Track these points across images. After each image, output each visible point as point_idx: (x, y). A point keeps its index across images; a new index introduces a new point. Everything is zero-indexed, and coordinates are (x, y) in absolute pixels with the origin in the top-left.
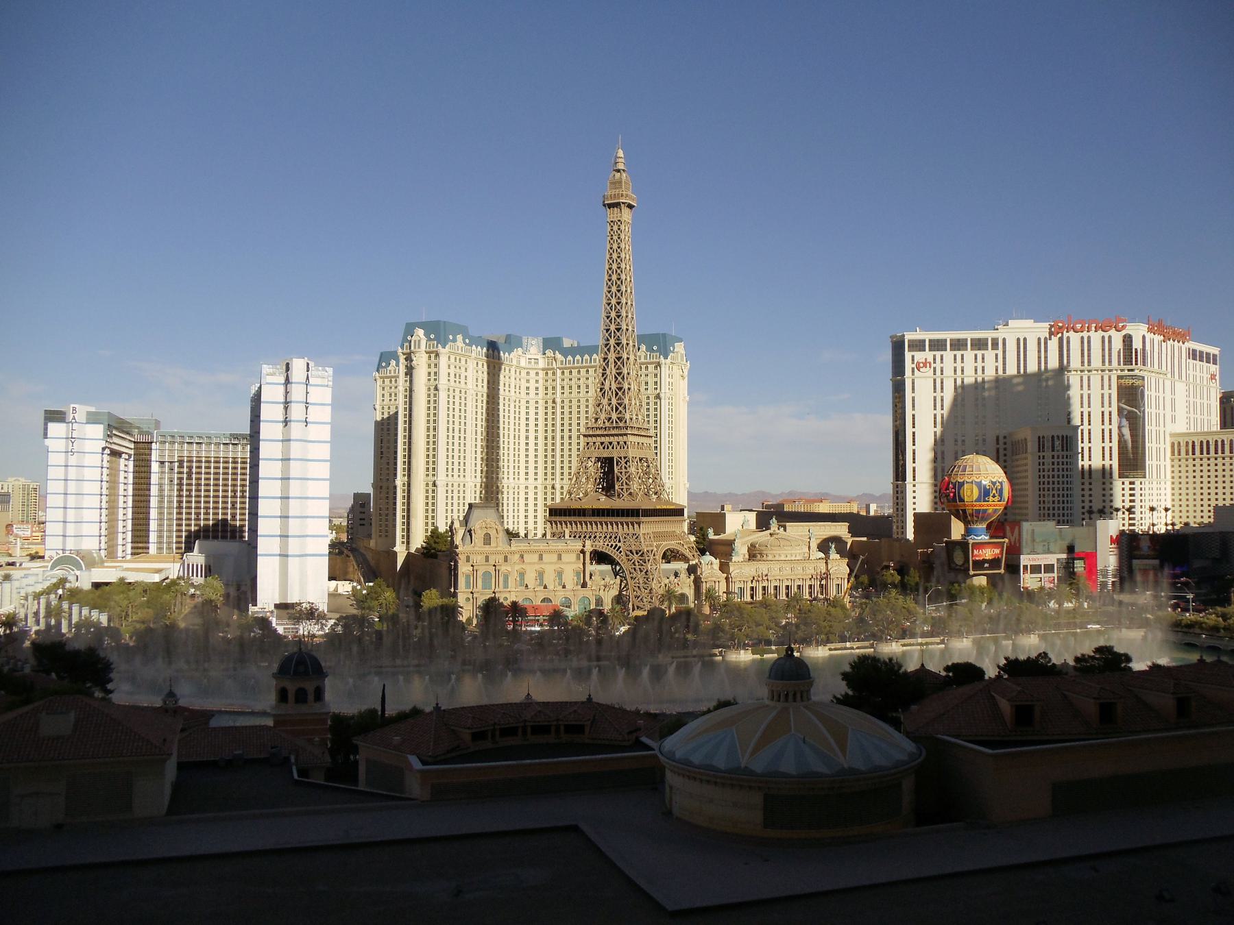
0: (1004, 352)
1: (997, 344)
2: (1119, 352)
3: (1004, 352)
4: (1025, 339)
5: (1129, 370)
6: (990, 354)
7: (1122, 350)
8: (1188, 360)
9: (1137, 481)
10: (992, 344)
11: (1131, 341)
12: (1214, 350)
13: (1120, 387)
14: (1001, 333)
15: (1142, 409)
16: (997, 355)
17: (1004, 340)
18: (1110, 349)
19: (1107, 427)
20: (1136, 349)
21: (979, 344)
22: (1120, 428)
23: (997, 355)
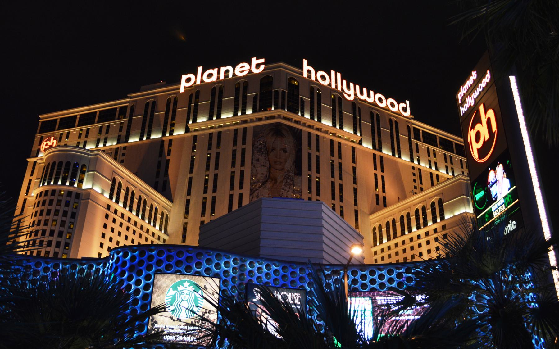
0: (130, 120)
2: (255, 97)
3: (130, 120)
5: (268, 118)
18: (245, 97)
19: (236, 192)
20: (277, 92)
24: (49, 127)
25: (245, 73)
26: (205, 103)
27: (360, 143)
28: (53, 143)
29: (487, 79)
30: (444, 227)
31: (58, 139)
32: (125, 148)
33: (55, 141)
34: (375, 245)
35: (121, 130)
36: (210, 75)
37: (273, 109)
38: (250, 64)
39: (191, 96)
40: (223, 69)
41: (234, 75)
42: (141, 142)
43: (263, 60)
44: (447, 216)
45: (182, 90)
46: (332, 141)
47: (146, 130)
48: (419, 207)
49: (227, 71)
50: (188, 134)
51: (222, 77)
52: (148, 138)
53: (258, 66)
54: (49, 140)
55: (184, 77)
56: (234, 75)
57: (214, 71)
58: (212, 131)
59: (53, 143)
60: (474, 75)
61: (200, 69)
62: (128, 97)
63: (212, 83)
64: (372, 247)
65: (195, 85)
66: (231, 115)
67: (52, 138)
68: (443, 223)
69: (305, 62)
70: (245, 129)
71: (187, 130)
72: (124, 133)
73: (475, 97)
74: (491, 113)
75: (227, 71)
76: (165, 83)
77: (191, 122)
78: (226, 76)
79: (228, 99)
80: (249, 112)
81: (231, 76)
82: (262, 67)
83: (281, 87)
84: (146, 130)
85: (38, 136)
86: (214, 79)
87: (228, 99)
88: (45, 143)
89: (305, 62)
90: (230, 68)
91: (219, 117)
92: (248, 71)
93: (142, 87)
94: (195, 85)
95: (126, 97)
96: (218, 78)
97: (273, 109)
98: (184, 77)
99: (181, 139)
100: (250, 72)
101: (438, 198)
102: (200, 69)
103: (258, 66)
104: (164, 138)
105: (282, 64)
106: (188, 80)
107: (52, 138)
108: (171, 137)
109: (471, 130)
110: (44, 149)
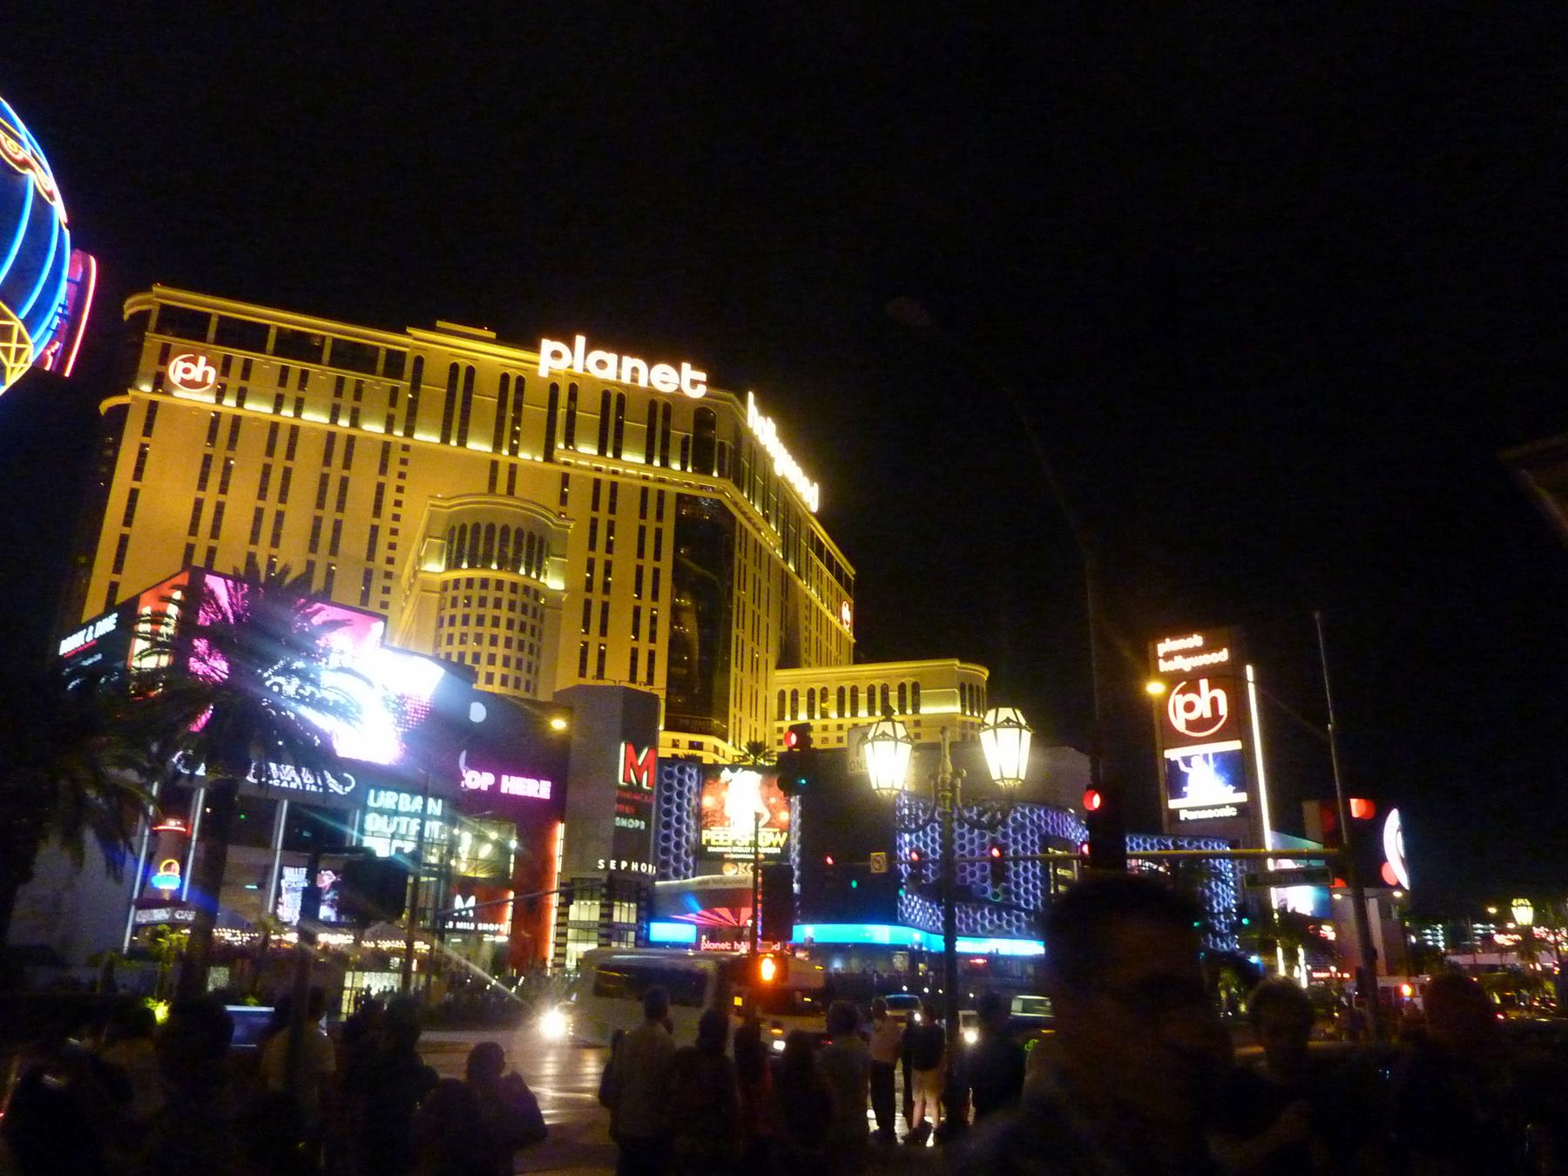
0: (415, 388)
1: (401, 365)
2: (685, 441)
4: (471, 371)
6: (378, 384)
7: (691, 440)
8: (809, 549)
9: (709, 741)
10: (388, 363)
11: (711, 425)
12: (850, 570)
13: (680, 521)
14: (414, 340)
15: (729, 583)
16: (394, 392)
17: (419, 361)
18: (666, 435)
20: (722, 445)
21: (352, 357)
22: (676, 611)
23: (394, 392)
24: (190, 326)
25: (669, 389)
26: (588, 415)
27: (775, 550)
28: (205, 374)
29: (1223, 656)
30: (917, 723)
31: (220, 366)
32: (406, 448)
33: (212, 372)
34: (781, 717)
35: (393, 402)
36: (601, 364)
37: (715, 474)
38: (678, 369)
39: (554, 388)
40: (629, 363)
41: (650, 383)
42: (444, 447)
43: (702, 376)
44: (926, 709)
45: (543, 372)
46: (756, 540)
47: (455, 425)
48: (878, 683)
49: (635, 370)
50: (548, 466)
52: (462, 442)
53: (694, 383)
54: (195, 363)
55: (548, 345)
56: (650, 383)
57: (611, 358)
58: (598, 475)
59: (205, 374)
60: (1197, 640)
61: (580, 341)
62: (409, 335)
63: (605, 382)
64: (775, 720)
65: (569, 370)
66: (641, 460)
67: (202, 360)
68: (916, 717)
69: (751, 396)
70: (661, 493)
71: (549, 457)
72: (401, 411)
73: (1195, 665)
74: (1220, 695)
75: (635, 370)
76: (493, 335)
77: (561, 445)
78: (634, 380)
79: (635, 425)
80: (676, 466)
81: (643, 383)
83: (722, 435)
84: (455, 425)
85: (153, 341)
86: (609, 374)
87: (635, 425)
88: (182, 365)
89: (751, 396)
90: (640, 363)
91: (617, 455)
92: (677, 387)
93: (440, 324)
94: (569, 370)
95: (403, 332)
96: (619, 377)
97: (715, 474)
98: (548, 345)
99: (532, 470)
100: (679, 389)
101: (913, 680)
102: (580, 341)
104: (497, 457)
105: (731, 395)
106: (556, 355)
107: (202, 360)
108: (513, 460)
109: (1178, 693)
110: (179, 380)
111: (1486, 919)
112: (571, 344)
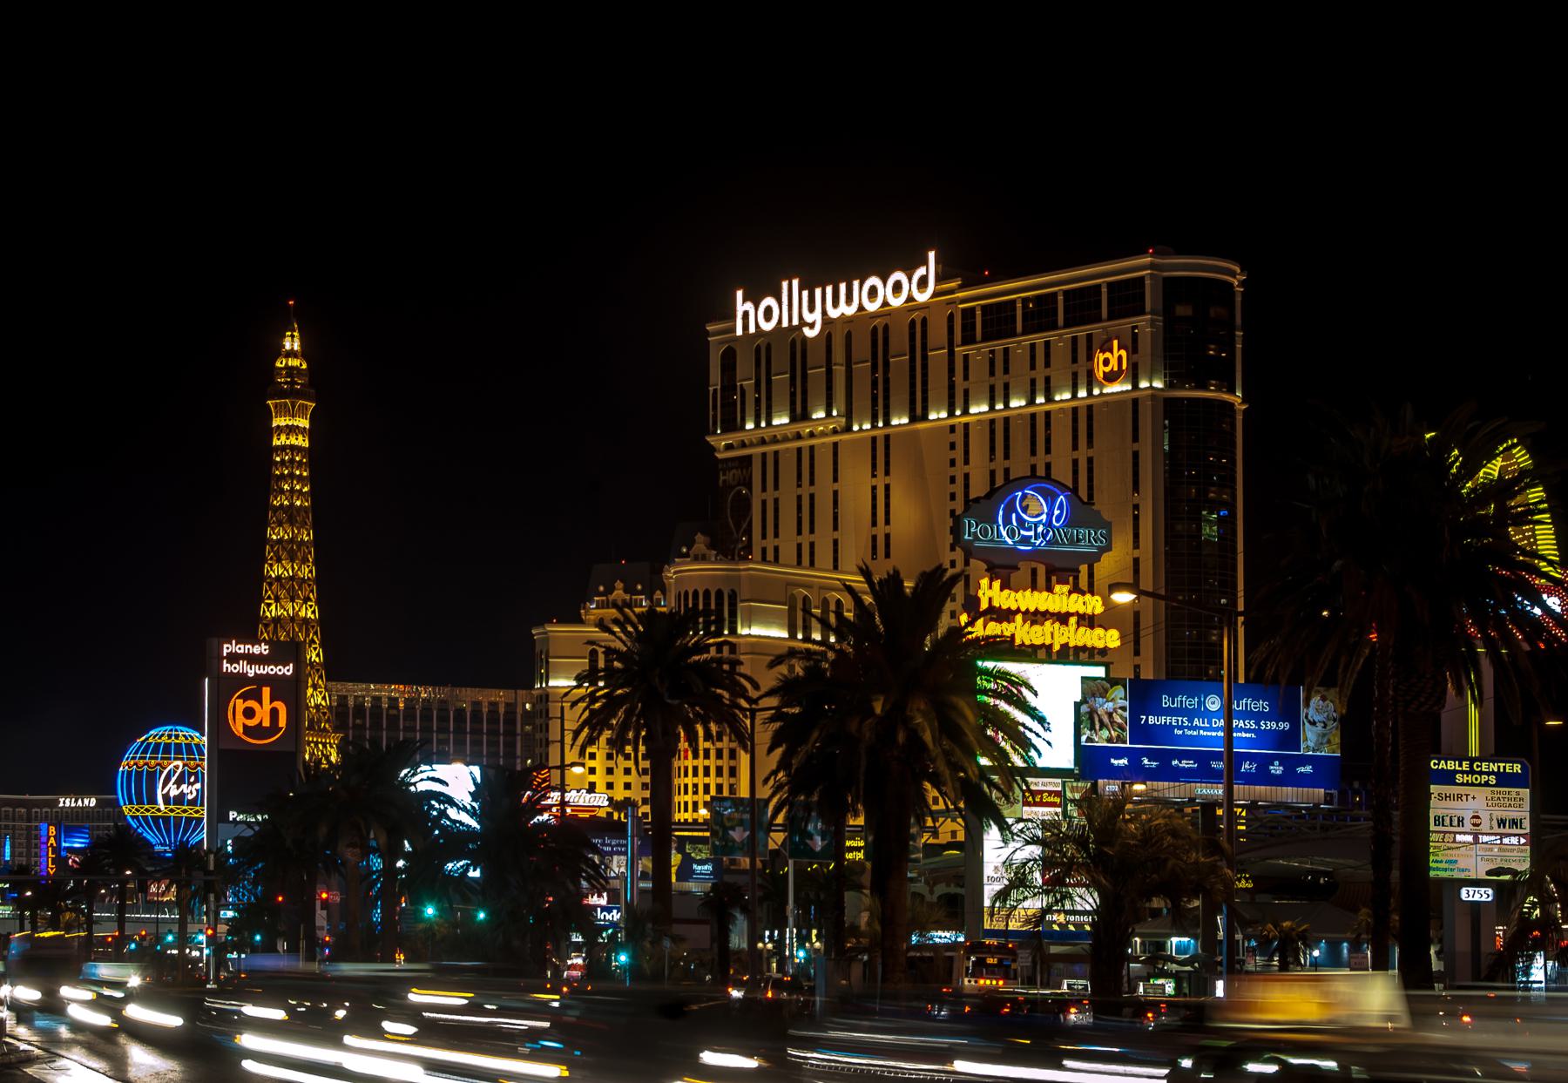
36: (240, 649)
40: (247, 647)
43: (267, 647)
49: (249, 649)
51: (246, 651)
53: (265, 650)
55: (225, 646)
57: (242, 646)
61: (234, 642)
75: (249, 649)
81: (251, 652)
82: (267, 651)
86: (242, 651)
90: (250, 646)
98: (225, 646)
102: (234, 642)
103: (265, 650)
111: (620, 656)
112: (231, 644)
